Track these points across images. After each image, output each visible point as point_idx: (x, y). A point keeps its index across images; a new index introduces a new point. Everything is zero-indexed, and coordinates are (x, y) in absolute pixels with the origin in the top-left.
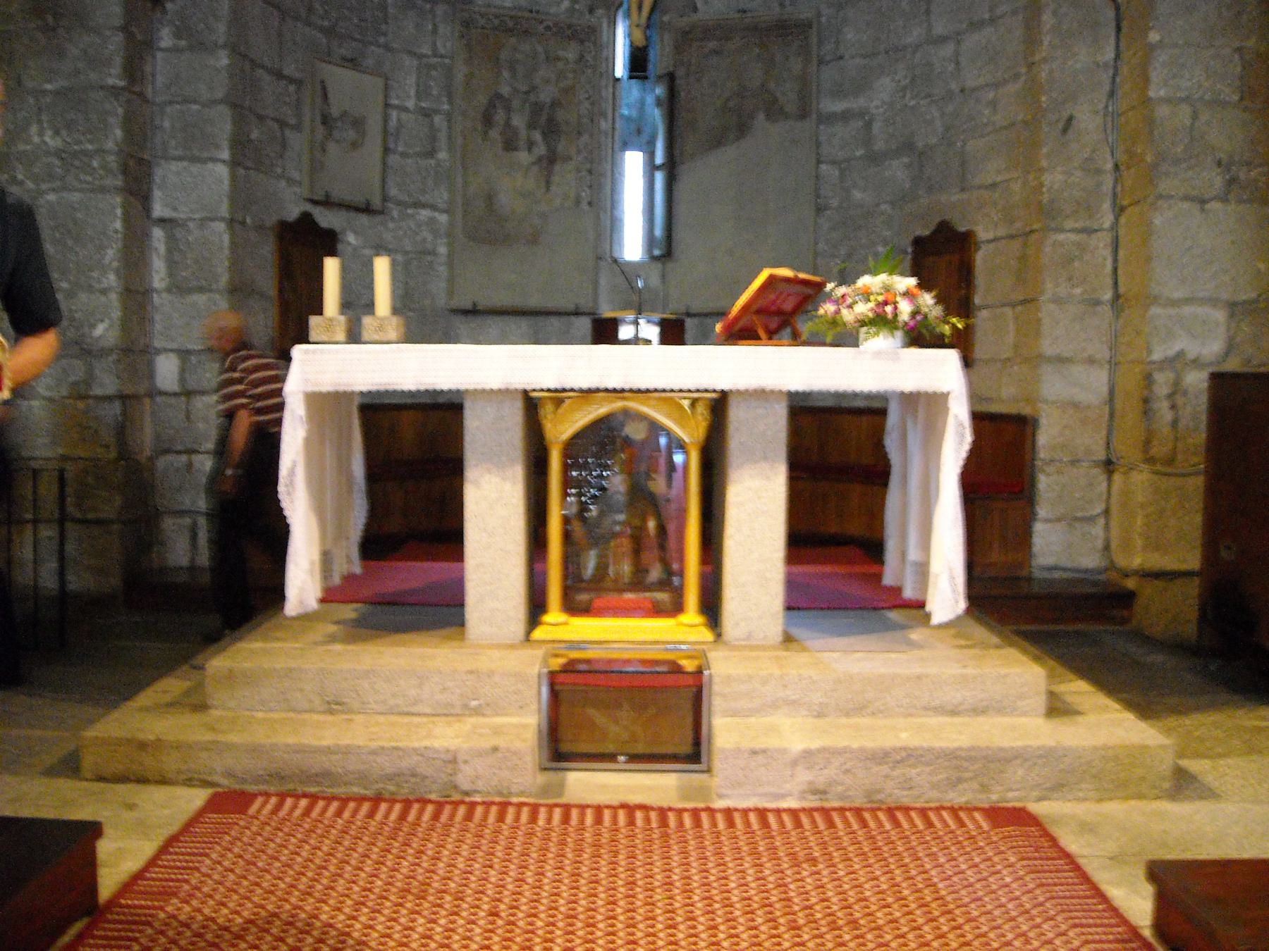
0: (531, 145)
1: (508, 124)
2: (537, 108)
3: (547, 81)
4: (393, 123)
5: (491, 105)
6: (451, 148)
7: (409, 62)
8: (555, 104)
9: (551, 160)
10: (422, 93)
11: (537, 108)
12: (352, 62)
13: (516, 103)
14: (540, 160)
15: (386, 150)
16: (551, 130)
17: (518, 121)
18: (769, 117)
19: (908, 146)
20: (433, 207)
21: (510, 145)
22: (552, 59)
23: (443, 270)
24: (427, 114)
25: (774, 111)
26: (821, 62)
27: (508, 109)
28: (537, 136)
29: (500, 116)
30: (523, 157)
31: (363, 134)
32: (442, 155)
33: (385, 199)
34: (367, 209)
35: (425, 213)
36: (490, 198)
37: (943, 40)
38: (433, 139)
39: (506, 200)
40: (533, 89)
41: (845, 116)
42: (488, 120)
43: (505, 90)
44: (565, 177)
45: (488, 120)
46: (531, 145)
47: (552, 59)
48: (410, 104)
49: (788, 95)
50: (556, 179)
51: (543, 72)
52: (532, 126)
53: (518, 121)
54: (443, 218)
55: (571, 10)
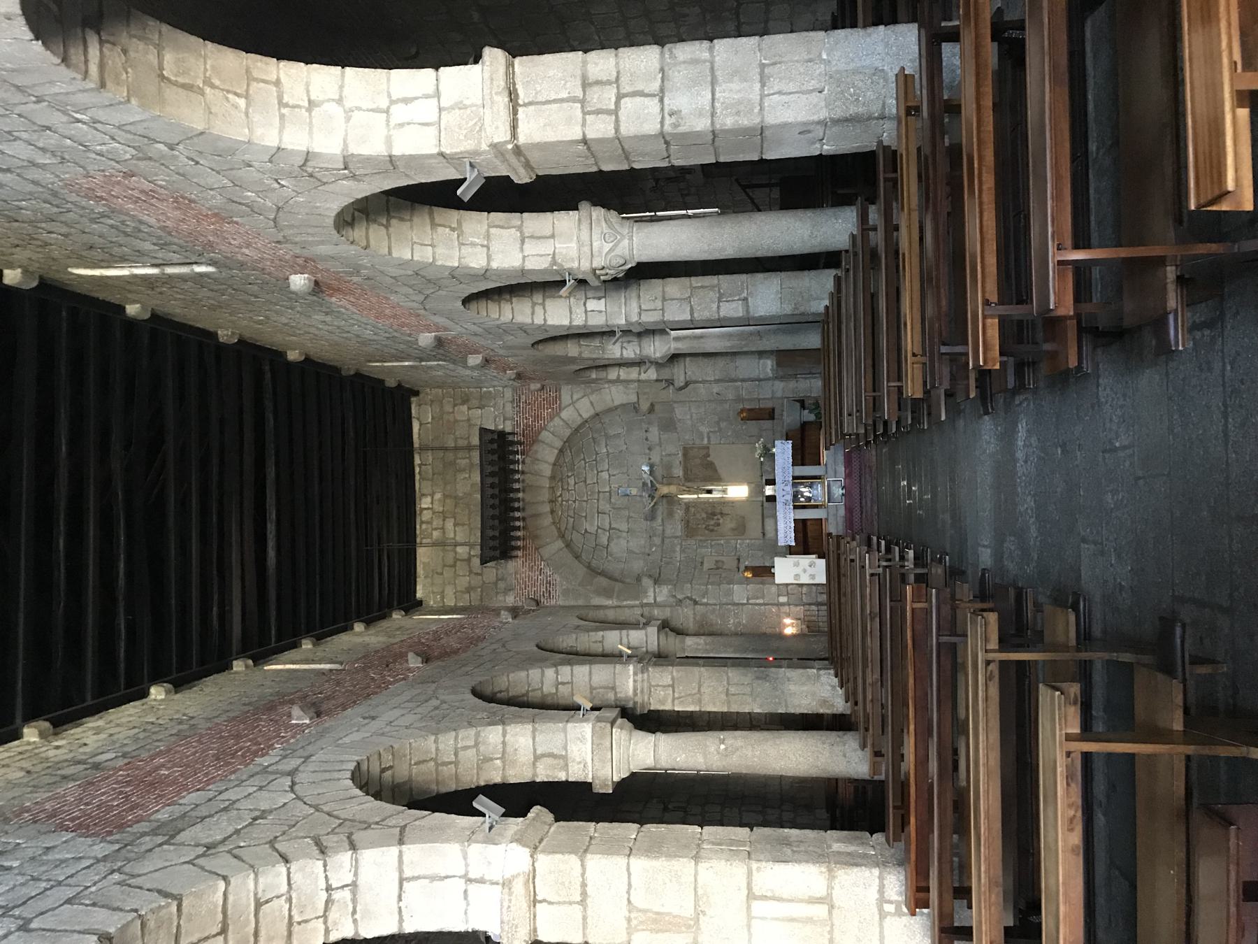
8: (706, 513)
12: (702, 563)
16: (714, 514)
17: (712, 522)
18: (709, 456)
19: (718, 423)
24: (712, 546)
29: (711, 527)
30: (721, 521)
34: (739, 560)
36: (733, 530)
39: (733, 525)
41: (709, 438)
42: (712, 531)
45: (712, 531)
49: (704, 452)
51: (698, 516)
53: (712, 522)
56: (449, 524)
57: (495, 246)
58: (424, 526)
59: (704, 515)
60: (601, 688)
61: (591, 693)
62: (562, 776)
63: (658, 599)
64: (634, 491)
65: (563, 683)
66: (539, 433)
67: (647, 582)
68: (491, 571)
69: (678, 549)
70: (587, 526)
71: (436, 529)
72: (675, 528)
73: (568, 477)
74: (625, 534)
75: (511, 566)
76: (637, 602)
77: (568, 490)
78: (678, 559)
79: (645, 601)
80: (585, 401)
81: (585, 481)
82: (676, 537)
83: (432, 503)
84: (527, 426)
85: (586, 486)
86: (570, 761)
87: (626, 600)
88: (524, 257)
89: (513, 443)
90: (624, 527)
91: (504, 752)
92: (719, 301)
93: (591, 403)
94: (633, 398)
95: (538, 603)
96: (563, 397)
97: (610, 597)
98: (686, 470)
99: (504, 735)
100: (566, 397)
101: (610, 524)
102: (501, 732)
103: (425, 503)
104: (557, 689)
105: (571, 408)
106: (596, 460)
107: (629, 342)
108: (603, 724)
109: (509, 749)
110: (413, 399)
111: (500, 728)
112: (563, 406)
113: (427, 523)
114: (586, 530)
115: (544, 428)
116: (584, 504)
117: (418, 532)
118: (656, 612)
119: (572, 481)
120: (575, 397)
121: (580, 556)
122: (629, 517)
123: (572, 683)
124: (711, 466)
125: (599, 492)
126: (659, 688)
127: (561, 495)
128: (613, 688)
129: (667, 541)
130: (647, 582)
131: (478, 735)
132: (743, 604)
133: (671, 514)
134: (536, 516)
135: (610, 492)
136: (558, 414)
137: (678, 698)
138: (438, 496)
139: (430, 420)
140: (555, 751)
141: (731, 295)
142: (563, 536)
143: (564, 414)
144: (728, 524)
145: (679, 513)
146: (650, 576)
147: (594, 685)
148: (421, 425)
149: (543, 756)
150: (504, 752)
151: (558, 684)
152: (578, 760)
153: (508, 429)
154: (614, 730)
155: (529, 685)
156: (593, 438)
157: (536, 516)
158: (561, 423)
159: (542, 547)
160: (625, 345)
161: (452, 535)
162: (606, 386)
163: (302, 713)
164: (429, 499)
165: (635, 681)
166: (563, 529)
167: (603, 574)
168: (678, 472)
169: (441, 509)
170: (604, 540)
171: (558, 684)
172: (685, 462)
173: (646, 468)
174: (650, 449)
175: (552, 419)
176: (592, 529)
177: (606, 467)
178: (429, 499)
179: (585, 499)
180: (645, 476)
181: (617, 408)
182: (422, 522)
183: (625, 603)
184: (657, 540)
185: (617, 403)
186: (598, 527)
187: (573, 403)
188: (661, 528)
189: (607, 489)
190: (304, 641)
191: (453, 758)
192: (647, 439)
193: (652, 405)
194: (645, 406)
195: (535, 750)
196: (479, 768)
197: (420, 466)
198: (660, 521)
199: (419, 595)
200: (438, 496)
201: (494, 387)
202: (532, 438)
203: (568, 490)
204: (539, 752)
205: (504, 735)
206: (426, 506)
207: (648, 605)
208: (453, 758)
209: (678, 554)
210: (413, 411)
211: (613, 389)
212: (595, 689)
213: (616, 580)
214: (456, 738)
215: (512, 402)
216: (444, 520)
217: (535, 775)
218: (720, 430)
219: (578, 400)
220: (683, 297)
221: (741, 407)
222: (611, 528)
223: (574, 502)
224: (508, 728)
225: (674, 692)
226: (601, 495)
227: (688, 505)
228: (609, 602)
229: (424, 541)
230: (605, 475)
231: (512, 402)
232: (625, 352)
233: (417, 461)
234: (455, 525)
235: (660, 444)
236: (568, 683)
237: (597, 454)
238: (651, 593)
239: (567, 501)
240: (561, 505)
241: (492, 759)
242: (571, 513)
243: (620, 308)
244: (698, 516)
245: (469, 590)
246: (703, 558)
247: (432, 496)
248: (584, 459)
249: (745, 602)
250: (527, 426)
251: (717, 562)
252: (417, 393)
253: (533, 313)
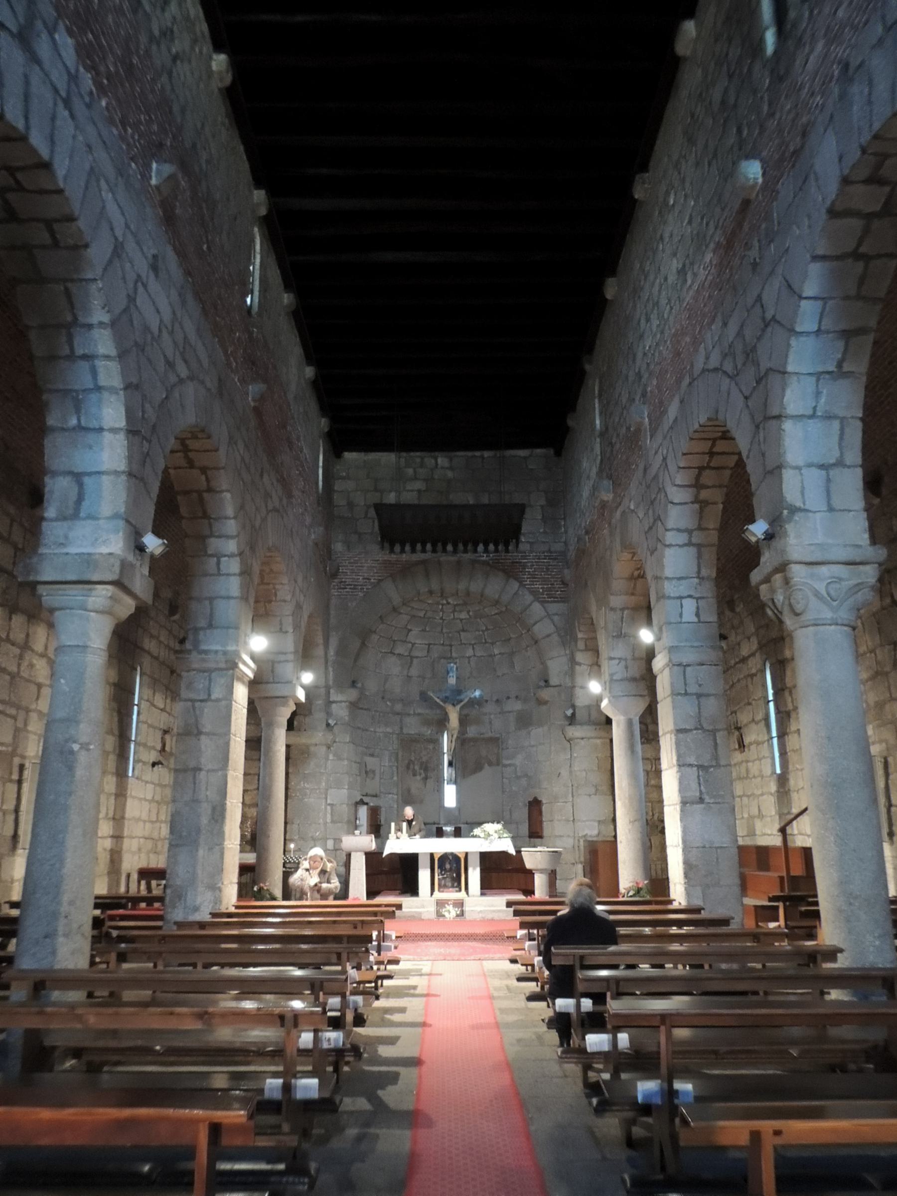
0: (420, 774)
1: (414, 769)
2: (422, 763)
3: (424, 755)
4: (382, 770)
5: (409, 764)
6: (398, 776)
7: (386, 753)
9: (426, 778)
10: (390, 760)
11: (422, 763)
12: (372, 755)
13: (416, 762)
14: (423, 779)
15: (381, 779)
16: (426, 769)
17: (417, 767)
19: (526, 775)
20: (393, 794)
21: (414, 775)
22: (426, 749)
23: (395, 812)
25: (490, 764)
26: (502, 749)
27: (414, 764)
28: (422, 771)
30: (418, 778)
31: (375, 775)
32: (395, 778)
33: (381, 792)
34: (376, 796)
35: (390, 796)
37: (533, 746)
38: (393, 774)
39: (414, 791)
40: (421, 758)
41: (510, 765)
42: (408, 768)
43: (413, 759)
44: (430, 783)
46: (420, 774)
47: (426, 749)
48: (387, 764)
50: (427, 784)
51: (424, 753)
52: (421, 769)
53: (417, 767)
54: (396, 797)
55: (431, 733)
56: (419, 485)
57: (814, 426)
58: (418, 460)
59: (424, 759)
60: (212, 609)
61: (206, 599)
62: (50, 512)
63: (334, 705)
64: (452, 681)
65: (218, 563)
66: (516, 579)
67: (353, 695)
68: (371, 526)
69: (389, 730)
70: (415, 631)
71: (415, 472)
72: (413, 727)
73: (468, 612)
74: (405, 672)
75: (376, 548)
76: (331, 683)
77: (454, 611)
78: (378, 730)
79: (332, 691)
80: (551, 629)
81: (463, 630)
82: (401, 728)
83: (442, 468)
84: (524, 566)
85: (459, 632)
86: (70, 523)
87: (333, 671)
88: (798, 468)
89: (507, 545)
90: (414, 672)
91: (87, 429)
92: (699, 767)
93: (548, 636)
94: (554, 681)
95: (334, 575)
96: (555, 605)
97: (337, 653)
98: (474, 740)
99: (113, 430)
100: (554, 608)
101: (417, 657)
102: (117, 426)
103: (442, 460)
104: (212, 556)
105: (543, 613)
106: (486, 642)
107: (626, 667)
108: (117, 569)
109: (91, 437)
110: (551, 451)
111: (122, 423)
112: (546, 605)
113: (422, 465)
114: (410, 630)
115: (522, 584)
116: (439, 629)
117: (412, 454)
118: (320, 702)
119: (463, 615)
120: (556, 618)
121: (383, 623)
122: (424, 678)
123: (219, 574)
124: (478, 768)
125: (451, 646)
126: (207, 683)
127: (448, 603)
128: (210, 626)
129: (398, 718)
130: (353, 695)
131: (112, 390)
132: (326, 798)
133: (427, 723)
134: (427, 575)
135: (451, 658)
136: (537, 599)
137: (194, 707)
138: (450, 474)
139: (530, 467)
140: (85, 504)
141: (706, 781)
142: (404, 604)
143: (537, 607)
144: (415, 784)
145: (428, 732)
146: (360, 699)
147: (215, 602)
148: (525, 458)
149: (81, 485)
150: (87, 429)
151: (218, 556)
152: (71, 535)
153: (522, 547)
154: (109, 587)
155: (215, 519)
156: (509, 639)
157: (427, 575)
158: (528, 603)
159: (394, 581)
160: (623, 663)
161: (408, 487)
162: (568, 652)
163: (165, 175)
164: (447, 464)
165: (216, 652)
166: (413, 605)
167: (363, 644)
168: (472, 731)
169: (436, 477)
170: (400, 649)
171: (218, 556)
172: (483, 739)
173: (477, 693)
174: (497, 701)
175: (533, 592)
176: (411, 638)
177: (479, 654)
178: (447, 464)
179: (444, 631)
180: (469, 693)
181: (543, 663)
182: (422, 458)
183: (331, 669)
184: (398, 707)
185: (550, 663)
186: (413, 644)
187: (549, 615)
188: (412, 712)
189: (454, 655)
190: (292, 295)
191: (79, 352)
192: (508, 698)
193: (546, 703)
194: (545, 694)
195: (90, 474)
196: (66, 392)
197: (482, 457)
198: (420, 711)
199: (347, 455)
200: (450, 474)
201: (566, 532)
202: (511, 572)
203: (454, 611)
204: (86, 480)
205: (113, 430)
206: (439, 460)
207: (328, 694)
208: (79, 352)
209: (381, 730)
210: (538, 451)
211: (564, 660)
212: (211, 603)
213: (356, 660)
214: (107, 357)
215: (550, 551)
216: (424, 480)
217: (54, 474)
218: (518, 778)
219: (552, 620)
220: (703, 719)
221: (544, 801)
222: (412, 658)
223: (442, 618)
224: (121, 436)
225: (202, 701)
226: (449, 648)
227: (437, 743)
228: (332, 652)
229: (402, 460)
230: (470, 652)
231: (550, 551)
232: (617, 661)
233: (487, 454)
234: (419, 491)
235: (502, 713)
236: (219, 569)
237: (493, 644)
238: (340, 698)
239: (442, 610)
240: (438, 603)
241: (78, 411)
242: (429, 614)
243: (686, 641)
244: (424, 753)
245: (351, 505)
246: (378, 756)
247: (451, 468)
248: (487, 629)
249: (329, 802)
250: (524, 566)
251: (374, 772)
252: (558, 453)
253: (679, 530)
